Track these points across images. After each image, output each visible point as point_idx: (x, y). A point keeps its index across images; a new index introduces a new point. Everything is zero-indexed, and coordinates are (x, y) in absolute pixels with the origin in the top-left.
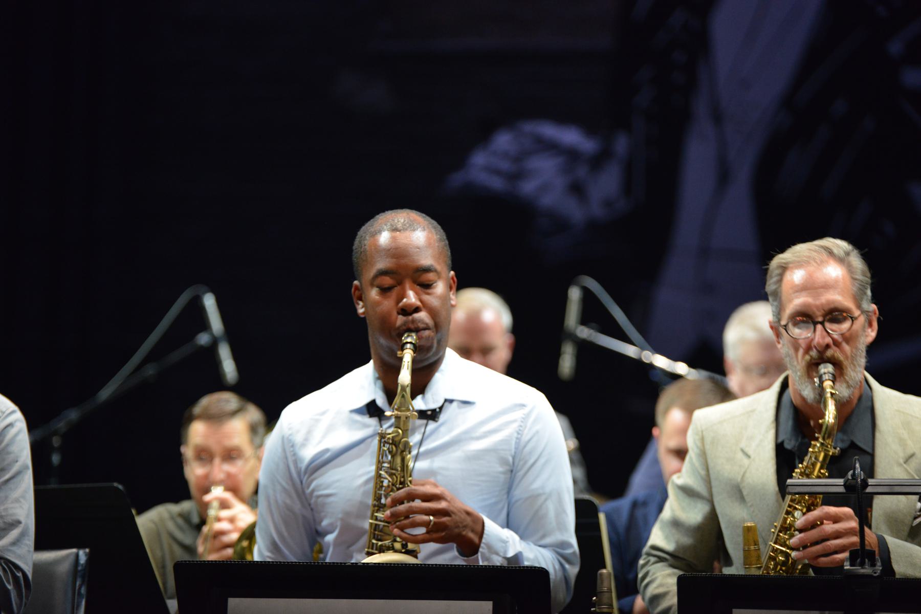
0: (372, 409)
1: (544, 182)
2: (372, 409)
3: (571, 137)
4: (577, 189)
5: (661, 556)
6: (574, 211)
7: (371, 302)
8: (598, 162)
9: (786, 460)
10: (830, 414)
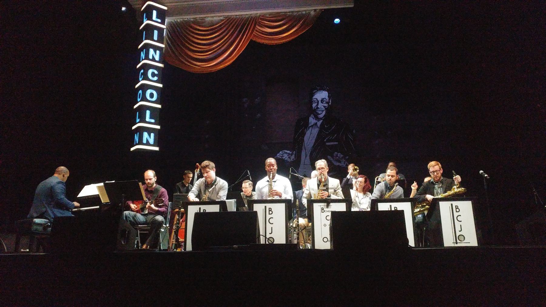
0: (268, 181)
1: (286, 157)
2: (268, 181)
3: (288, 152)
4: (289, 158)
5: (304, 198)
6: (289, 160)
7: (267, 168)
8: (292, 155)
9: (319, 185)
10: (323, 180)
